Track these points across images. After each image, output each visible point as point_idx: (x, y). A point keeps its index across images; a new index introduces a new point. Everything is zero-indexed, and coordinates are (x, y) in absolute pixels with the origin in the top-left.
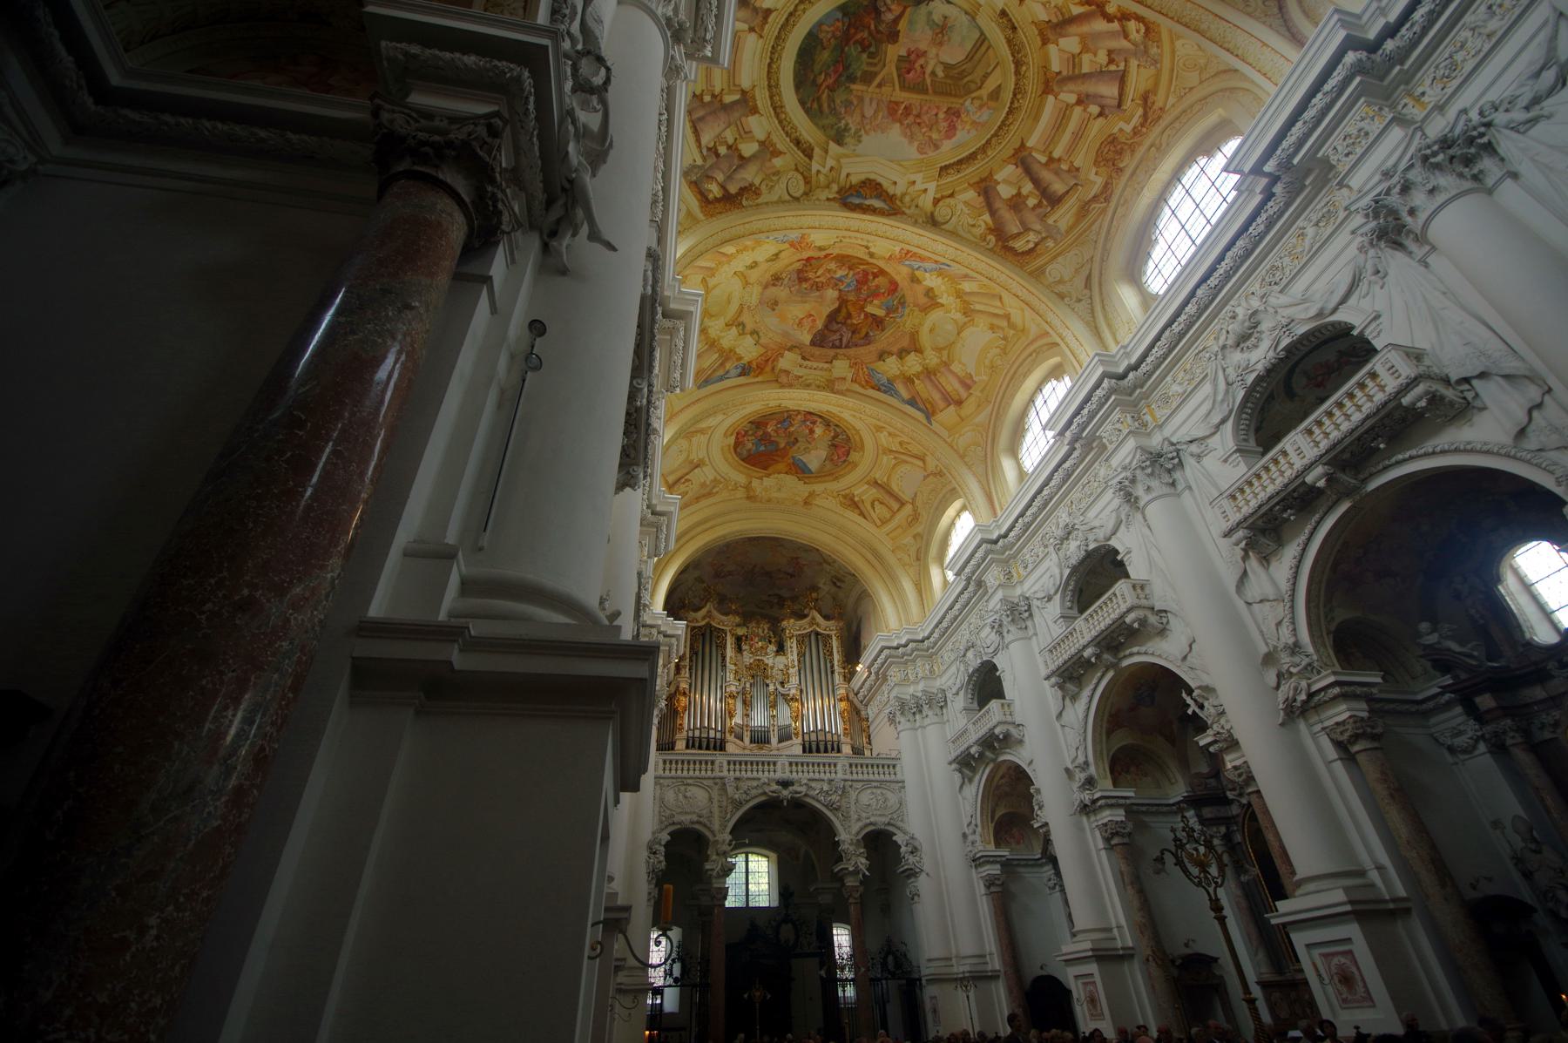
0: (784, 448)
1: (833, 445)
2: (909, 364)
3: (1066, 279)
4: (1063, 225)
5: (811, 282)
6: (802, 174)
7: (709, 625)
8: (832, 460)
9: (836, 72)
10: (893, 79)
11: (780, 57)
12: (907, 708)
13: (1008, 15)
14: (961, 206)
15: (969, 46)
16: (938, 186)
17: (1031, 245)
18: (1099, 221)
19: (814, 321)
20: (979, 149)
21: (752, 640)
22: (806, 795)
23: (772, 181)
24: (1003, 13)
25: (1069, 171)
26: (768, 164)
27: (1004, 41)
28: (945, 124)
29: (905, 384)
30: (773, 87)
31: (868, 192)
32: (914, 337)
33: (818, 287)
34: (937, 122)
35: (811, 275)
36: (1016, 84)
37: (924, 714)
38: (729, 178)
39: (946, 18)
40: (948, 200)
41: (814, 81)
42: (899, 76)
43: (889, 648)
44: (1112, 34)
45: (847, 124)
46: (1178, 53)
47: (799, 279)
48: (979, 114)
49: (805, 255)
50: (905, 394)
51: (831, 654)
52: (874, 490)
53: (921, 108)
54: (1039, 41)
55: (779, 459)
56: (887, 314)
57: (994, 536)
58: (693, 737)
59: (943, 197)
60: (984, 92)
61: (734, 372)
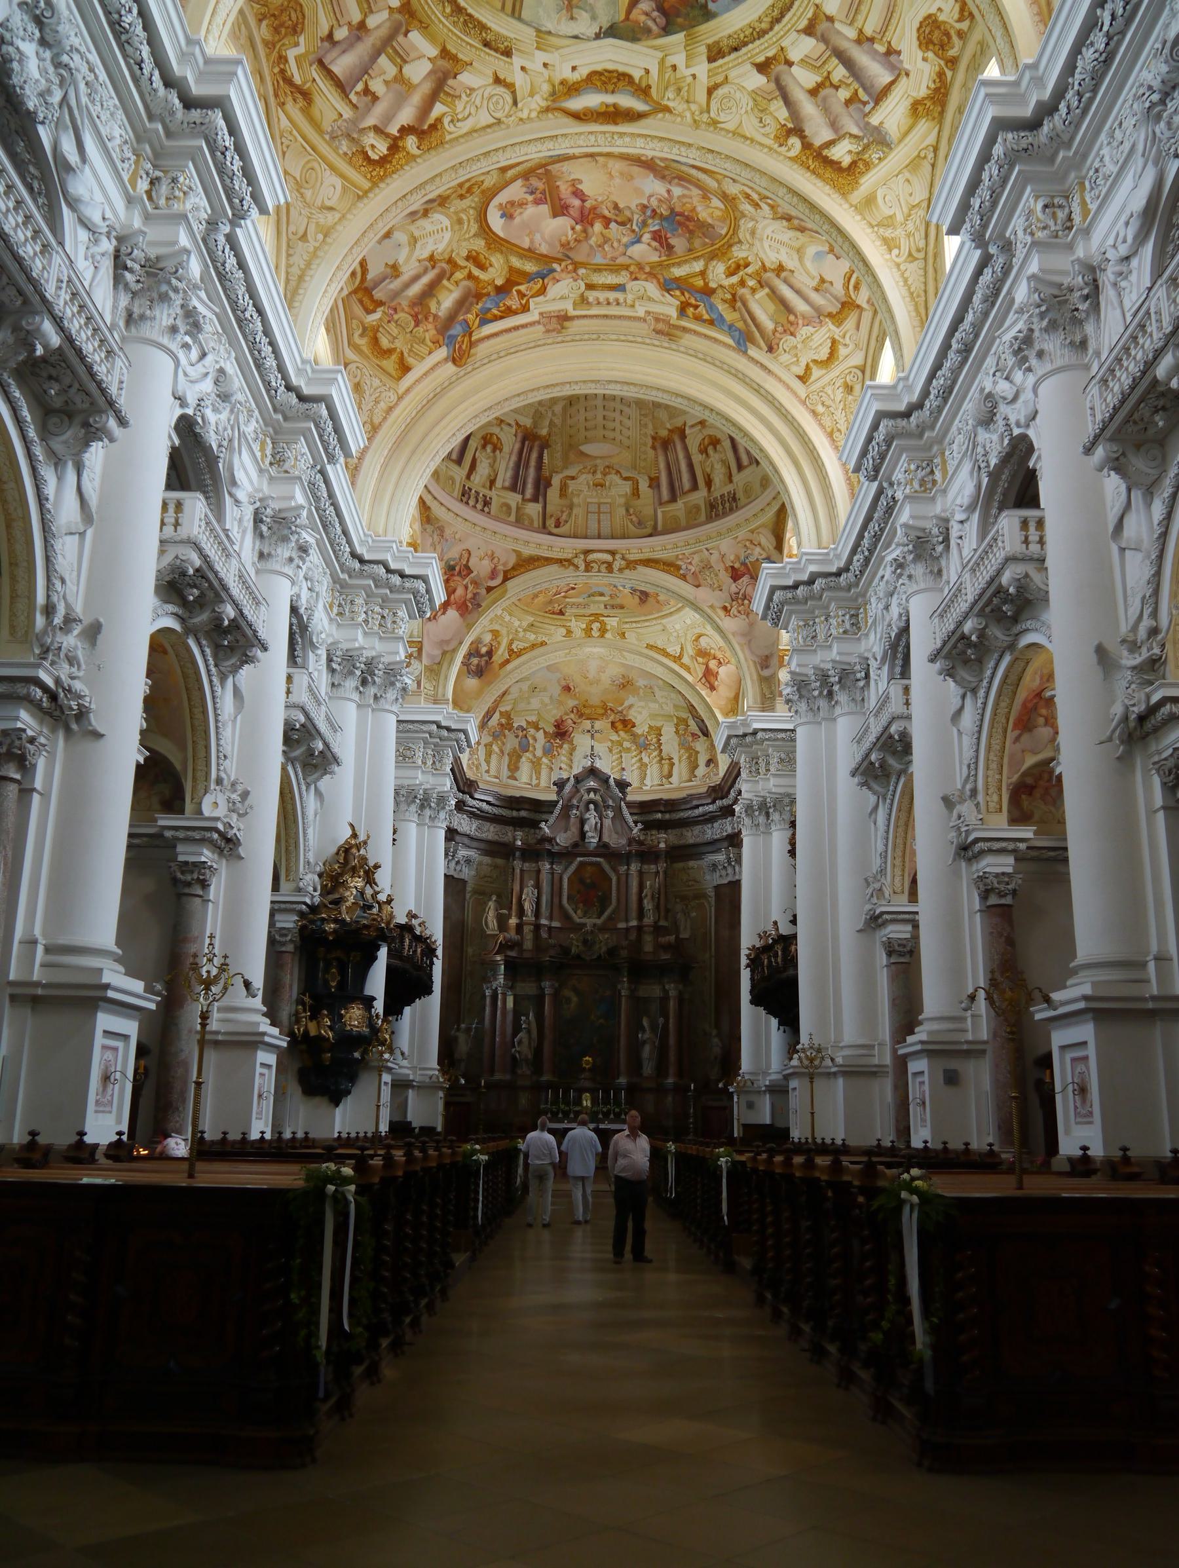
13: (502, 54)
24: (508, 53)
27: (489, 24)
39: (572, 18)
44: (389, 118)
46: (328, 172)
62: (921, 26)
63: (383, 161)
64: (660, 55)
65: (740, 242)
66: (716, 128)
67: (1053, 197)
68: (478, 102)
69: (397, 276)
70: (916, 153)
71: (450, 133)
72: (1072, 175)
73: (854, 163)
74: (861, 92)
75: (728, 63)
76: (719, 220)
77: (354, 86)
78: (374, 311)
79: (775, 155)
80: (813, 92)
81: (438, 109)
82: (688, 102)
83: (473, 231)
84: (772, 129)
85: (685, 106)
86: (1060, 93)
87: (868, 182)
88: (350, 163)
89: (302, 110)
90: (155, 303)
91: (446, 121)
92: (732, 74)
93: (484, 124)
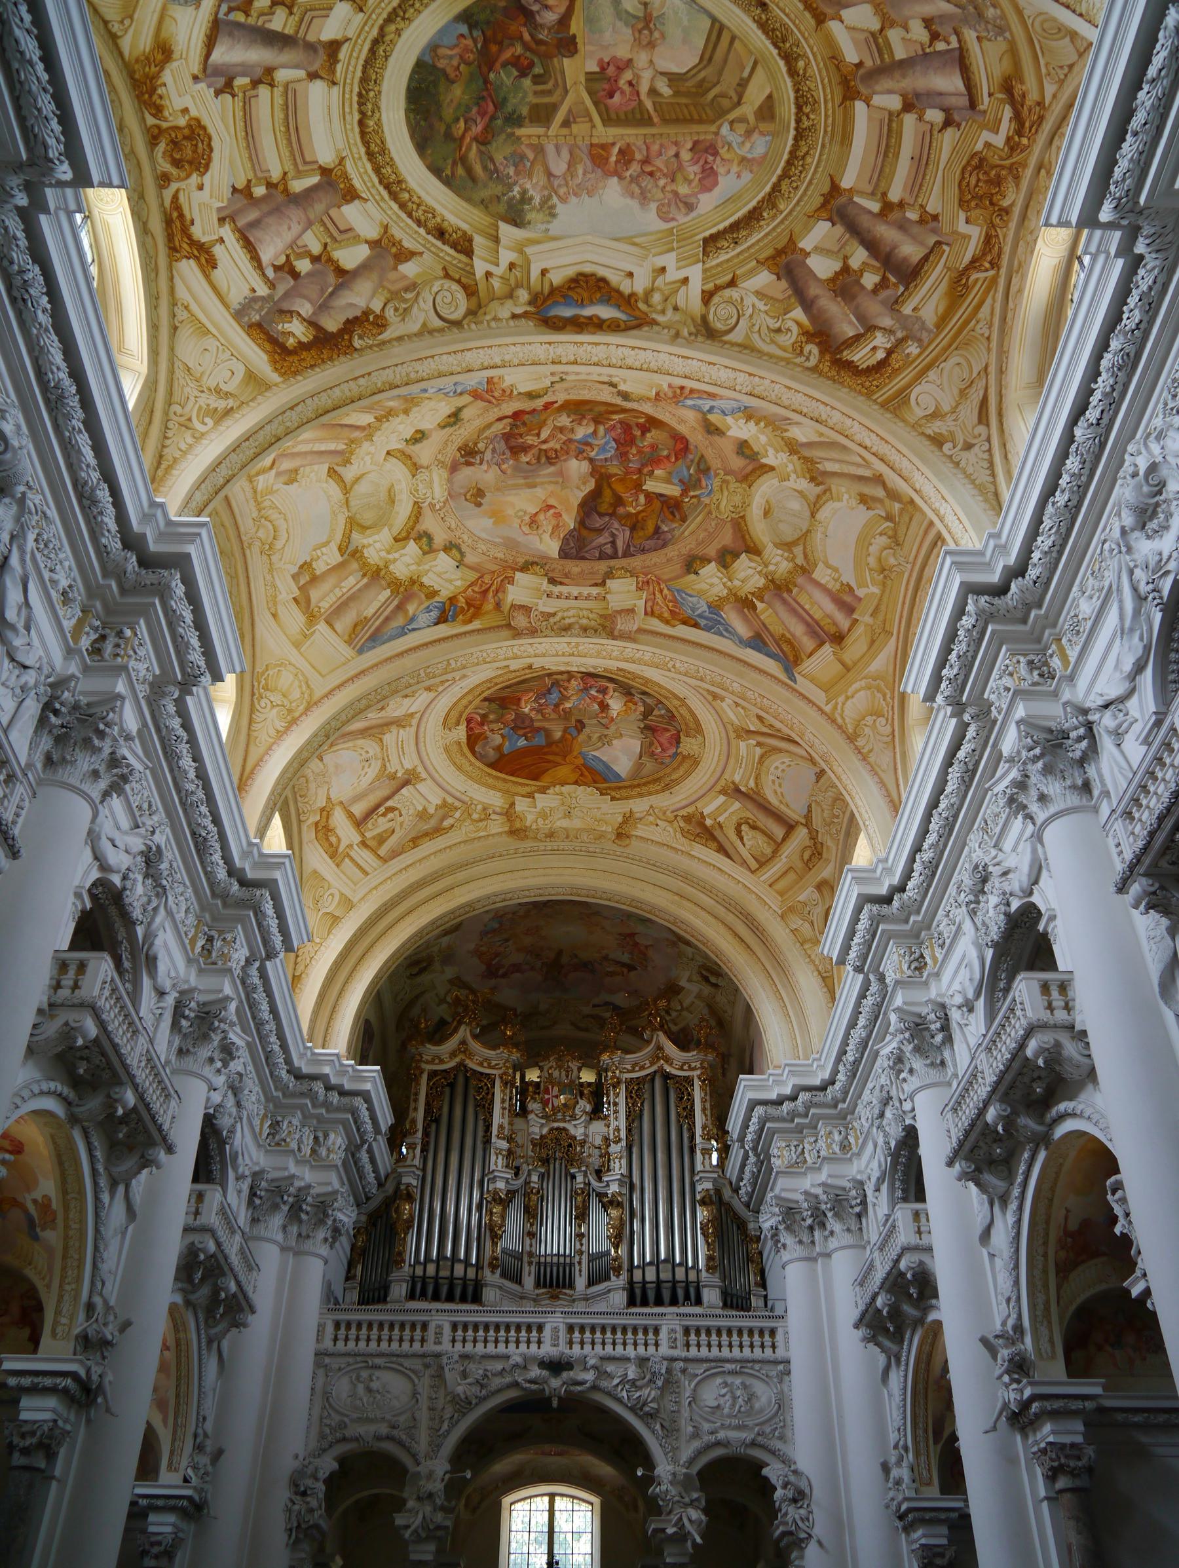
0: (563, 737)
1: (647, 727)
2: (742, 575)
3: (946, 408)
4: (929, 314)
5: (535, 451)
6: (459, 282)
7: (461, 1064)
8: (652, 754)
9: (482, 114)
10: (587, 110)
12: (798, 1217)
14: (750, 300)
15: (701, 44)
16: (705, 271)
17: (880, 355)
18: (989, 301)
19: (558, 515)
20: (763, 201)
21: (547, 1091)
22: (595, 1387)
23: (405, 301)
25: (921, 221)
26: (392, 275)
27: (754, 26)
28: (697, 168)
29: (741, 612)
30: (377, 154)
31: (585, 295)
32: (739, 525)
33: (550, 458)
34: (680, 167)
35: (530, 440)
36: (797, 91)
37: (829, 1227)
38: (323, 307)
40: (727, 293)
41: (448, 136)
42: (596, 104)
43: (765, 1103)
45: (524, 192)
46: (1026, 13)
47: (511, 449)
48: (748, 145)
49: (509, 408)
50: (743, 630)
51: (691, 1115)
52: (737, 805)
53: (648, 149)
55: (558, 759)
56: (685, 492)
57: (883, 890)
58: (424, 1278)
59: (718, 288)
60: (748, 109)
61: (424, 619)
62: (209, 145)
74: (239, 17)
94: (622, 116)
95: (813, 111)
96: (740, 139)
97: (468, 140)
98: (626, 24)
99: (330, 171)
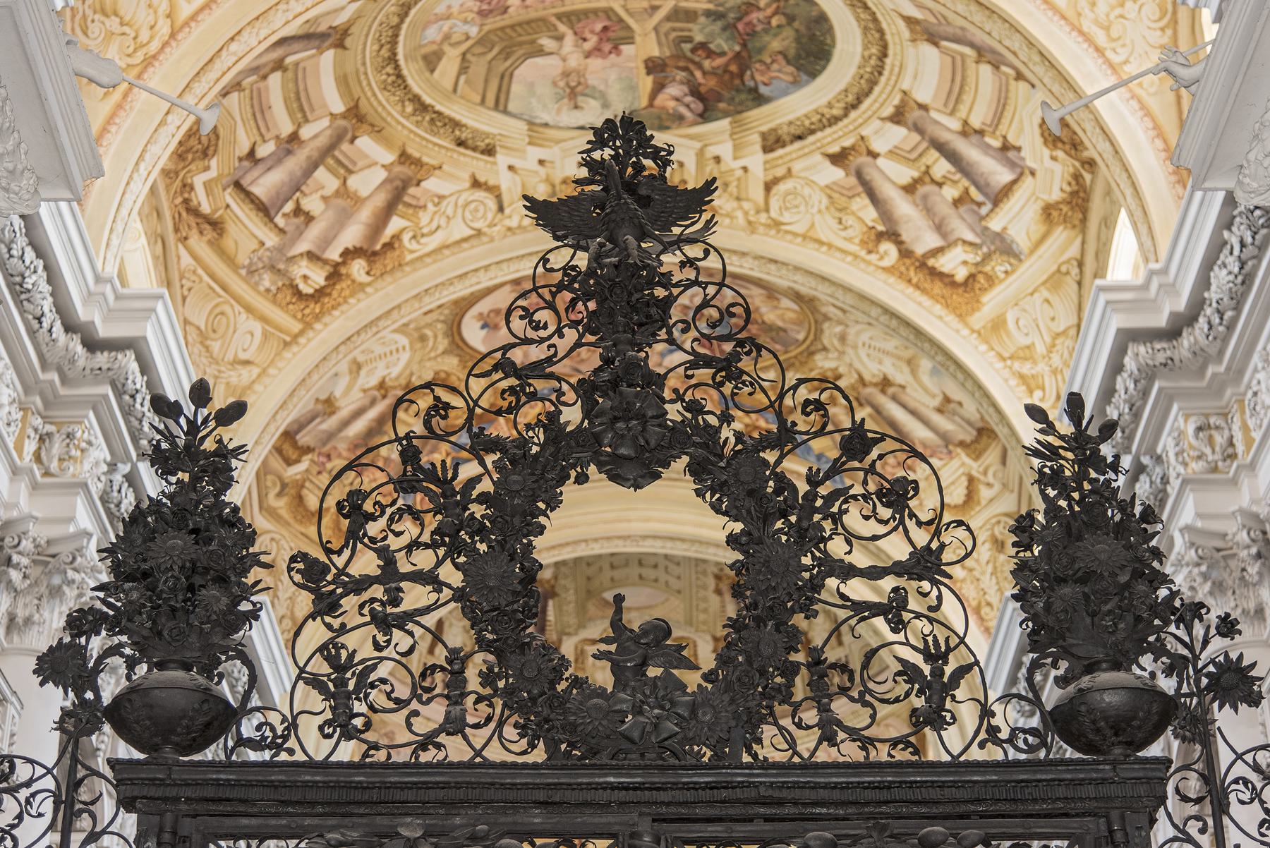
9: (749, 23)
11: (866, 59)
13: (483, 152)
15: (516, 88)
24: (490, 151)
25: (239, 84)
27: (464, 121)
30: (873, 28)
36: (405, 87)
39: (576, 107)
41: (791, 19)
42: (621, 20)
44: (327, 241)
46: (244, 316)
48: (445, 29)
54: (413, 151)
63: (320, 294)
64: (698, 145)
65: (825, 349)
66: (778, 231)
67: (1207, 416)
68: (450, 211)
69: (333, 413)
70: (1054, 268)
71: (412, 252)
72: (1229, 392)
73: (972, 277)
74: (974, 192)
75: (790, 153)
76: (794, 323)
77: (281, 207)
78: (298, 461)
79: (862, 265)
80: (909, 189)
81: (395, 224)
82: (738, 199)
83: (441, 348)
84: (856, 231)
85: (735, 204)
86: (1197, 305)
87: (992, 301)
88: (274, 301)
89: (210, 243)
90: (45, 600)
91: (406, 238)
92: (797, 167)
93: (457, 236)
94: (591, 15)
95: (385, 81)
96: (455, 29)
97: (769, 11)
98: (594, 88)
99: (927, 40)
